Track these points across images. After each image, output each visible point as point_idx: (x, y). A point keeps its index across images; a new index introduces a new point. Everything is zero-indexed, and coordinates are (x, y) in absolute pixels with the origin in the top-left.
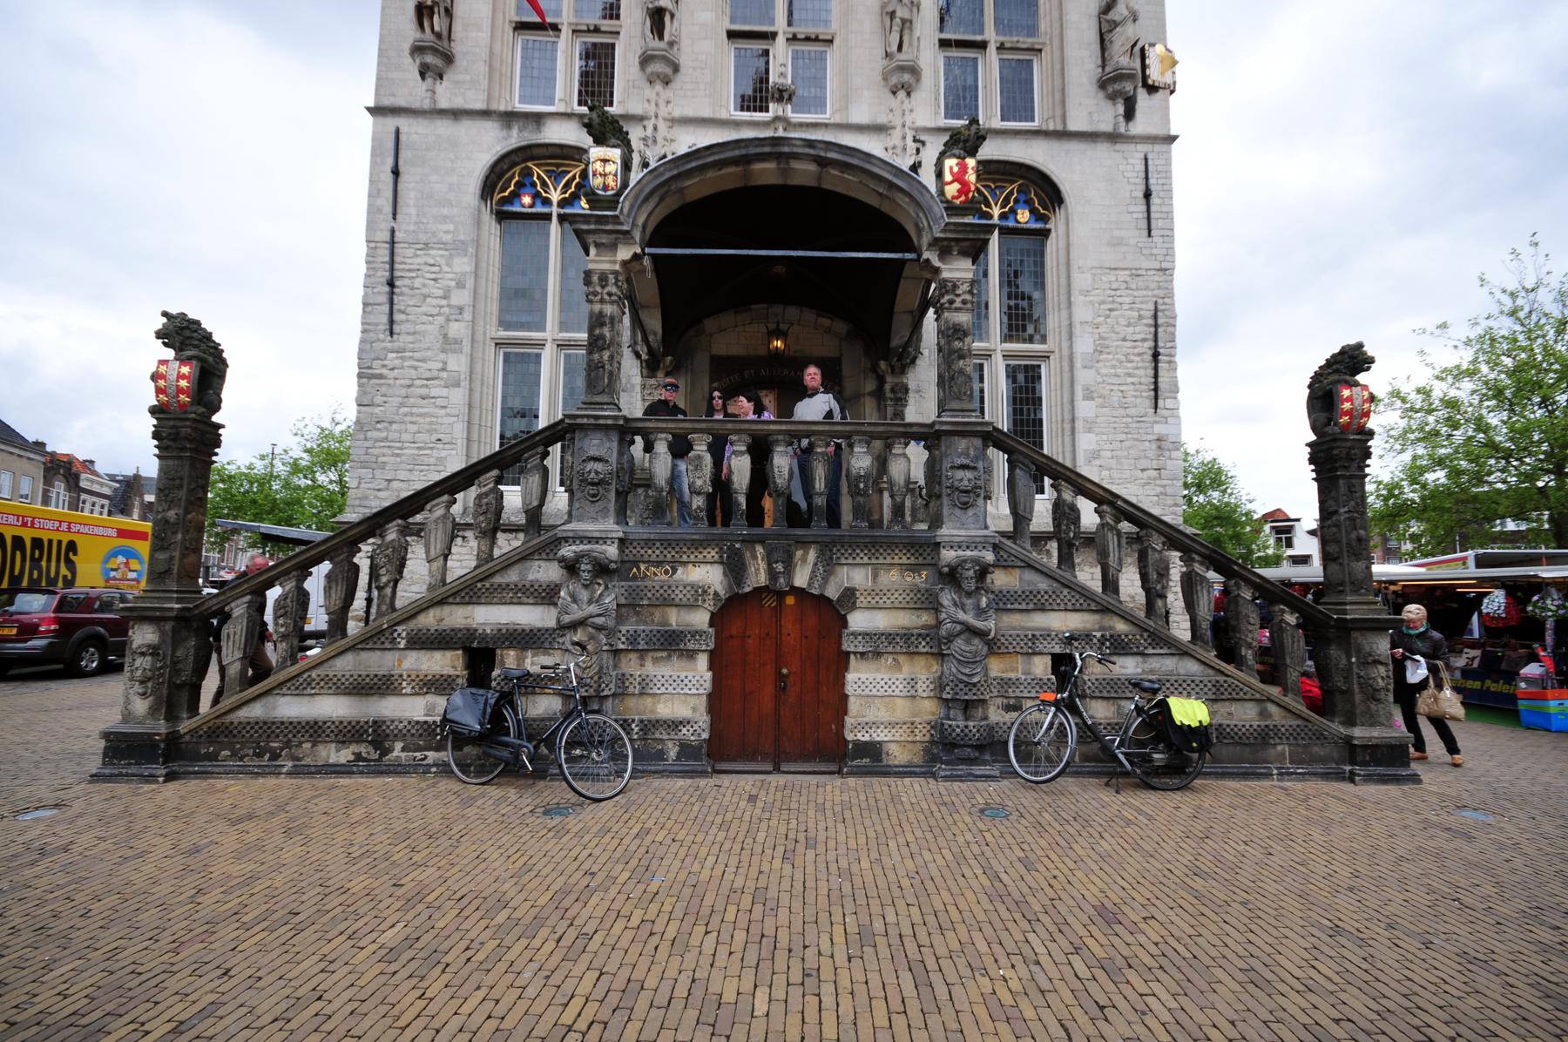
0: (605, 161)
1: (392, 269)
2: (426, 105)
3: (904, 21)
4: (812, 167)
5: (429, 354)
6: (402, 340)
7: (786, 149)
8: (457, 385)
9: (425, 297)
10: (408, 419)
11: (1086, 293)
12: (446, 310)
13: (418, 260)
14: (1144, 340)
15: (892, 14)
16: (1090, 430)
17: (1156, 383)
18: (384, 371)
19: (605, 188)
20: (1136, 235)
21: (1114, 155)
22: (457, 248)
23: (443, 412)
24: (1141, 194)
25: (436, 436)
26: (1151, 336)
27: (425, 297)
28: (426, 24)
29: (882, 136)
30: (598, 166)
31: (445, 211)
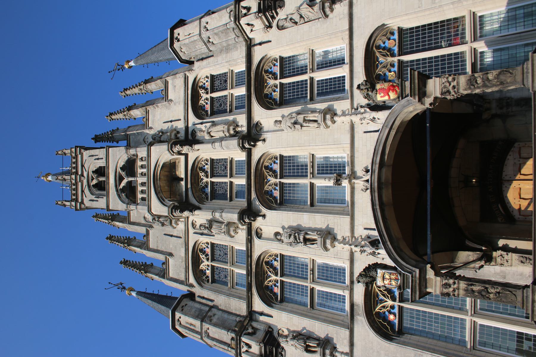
0: (384, 278)
4: (384, 170)
7: (376, 184)
29: (355, 126)
30: (386, 282)
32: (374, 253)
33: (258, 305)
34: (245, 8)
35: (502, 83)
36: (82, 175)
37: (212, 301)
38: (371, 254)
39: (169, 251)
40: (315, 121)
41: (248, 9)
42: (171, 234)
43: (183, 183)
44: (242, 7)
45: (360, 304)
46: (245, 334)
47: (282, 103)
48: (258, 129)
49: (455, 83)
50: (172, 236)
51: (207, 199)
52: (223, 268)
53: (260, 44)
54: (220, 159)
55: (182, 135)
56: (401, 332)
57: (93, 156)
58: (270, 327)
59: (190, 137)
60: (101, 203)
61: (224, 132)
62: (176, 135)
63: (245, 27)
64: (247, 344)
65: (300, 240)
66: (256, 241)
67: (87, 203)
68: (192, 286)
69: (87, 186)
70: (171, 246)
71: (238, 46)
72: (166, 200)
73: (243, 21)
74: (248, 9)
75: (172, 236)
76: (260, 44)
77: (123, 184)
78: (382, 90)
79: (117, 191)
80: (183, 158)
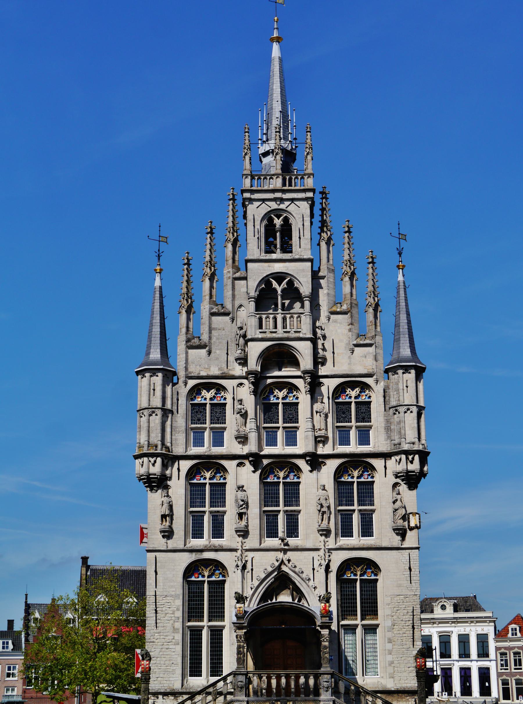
1: (156, 605)
2: (164, 548)
5: (168, 634)
6: (160, 629)
8: (178, 644)
9: (166, 614)
10: (163, 656)
11: (389, 604)
12: (173, 618)
13: (164, 601)
14: (409, 621)
16: (391, 654)
17: (413, 636)
18: (154, 640)
19: (240, 614)
20: (407, 583)
21: (398, 554)
22: (176, 597)
23: (174, 653)
24: (408, 568)
25: (171, 662)
26: (411, 619)
27: (166, 614)
28: (164, 520)
31: (172, 584)
32: (238, 566)
33: (186, 465)
34: (413, 458)
35: (324, 659)
36: (282, 200)
37: (178, 412)
38: (237, 564)
39: (213, 351)
40: (322, 520)
41: (412, 462)
42: (229, 353)
43: (276, 373)
44: (414, 456)
45: (203, 556)
49: (325, 640)
50: (227, 354)
51: (264, 399)
52: (206, 416)
53: (385, 467)
54: (298, 412)
56: (190, 583)
57: (303, 225)
58: (170, 478)
60: (254, 248)
61: (320, 430)
62: (320, 362)
63: (399, 457)
64: (155, 462)
65: (241, 509)
66: (236, 462)
67: (251, 209)
68: (186, 384)
69: (269, 209)
70: (218, 352)
71: (389, 441)
73: (403, 457)
74: (412, 462)
75: (227, 354)
76: (385, 467)
77: (275, 284)
78: (326, 606)
79: (267, 276)
80: (299, 373)
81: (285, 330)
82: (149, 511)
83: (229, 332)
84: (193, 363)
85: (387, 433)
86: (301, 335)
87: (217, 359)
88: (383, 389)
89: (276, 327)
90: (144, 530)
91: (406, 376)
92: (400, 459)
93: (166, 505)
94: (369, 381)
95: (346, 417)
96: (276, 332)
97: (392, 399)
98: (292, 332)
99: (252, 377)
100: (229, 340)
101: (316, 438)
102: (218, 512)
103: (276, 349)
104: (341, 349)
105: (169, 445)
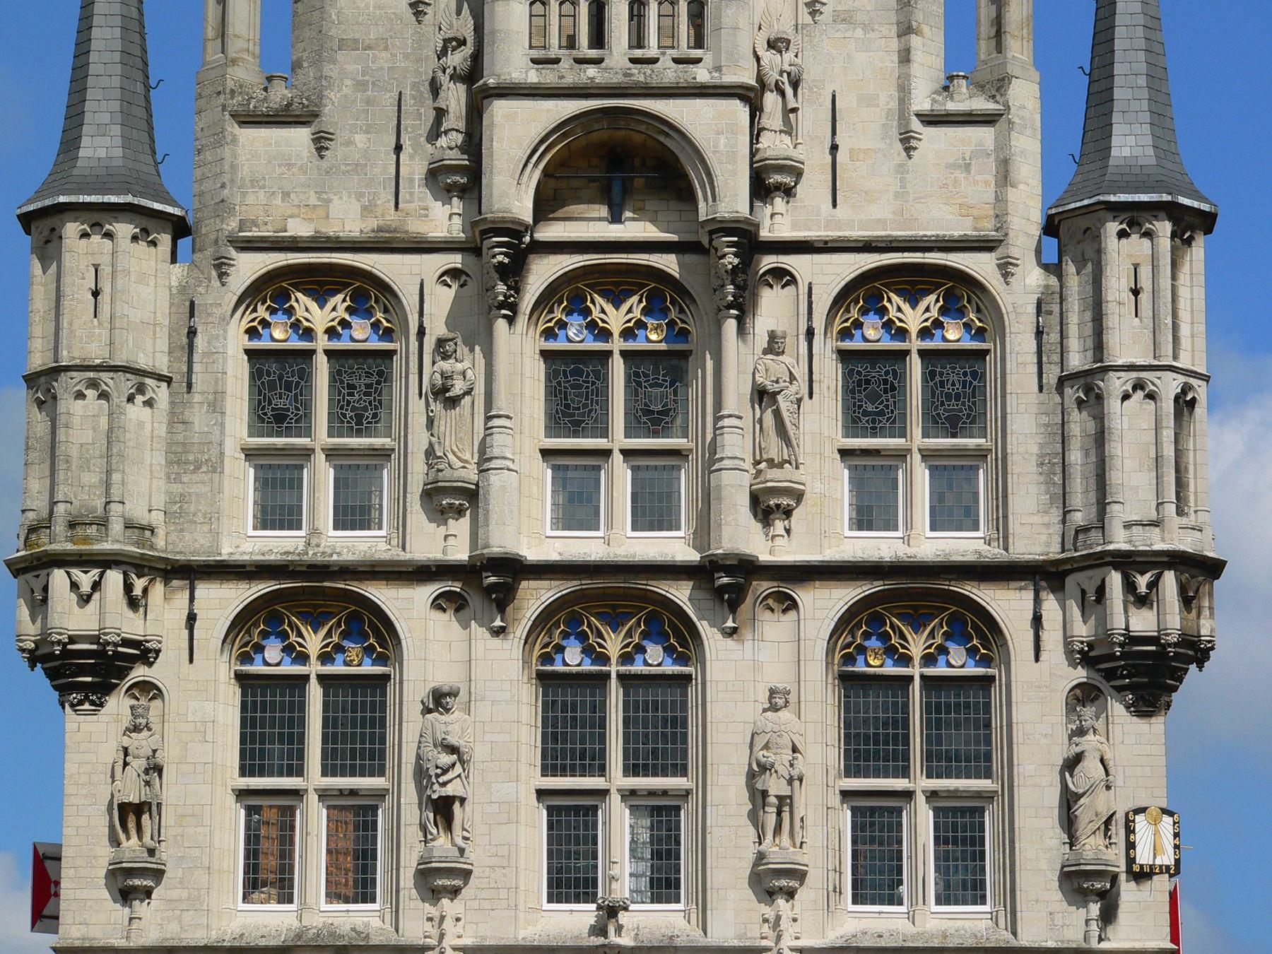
3: (780, 798)
15: (765, 794)
28: (132, 825)
33: (222, 602)
34: (1153, 585)
39: (341, 136)
42: (406, 141)
46: (125, 574)
47: (851, 683)
48: (770, 601)
50: (398, 148)
53: (1037, 620)
55: (778, 222)
58: (158, 652)
59: (768, 261)
62: (778, 187)
63: (1096, 574)
71: (1056, 515)
72: (537, 174)
75: (398, 148)
76: (1037, 620)
81: (638, 53)
82: (69, 789)
83: (406, 56)
84: (254, 182)
85: (1049, 482)
86: (702, 75)
87: (358, 168)
88: (1034, 298)
89: (598, 39)
90: (48, 864)
91: (1137, 246)
92: (1101, 591)
93: (138, 764)
94: (980, 265)
95: (881, 413)
96: (598, 61)
97: (1074, 343)
98: (666, 62)
99: (500, 245)
100: (408, 92)
101: (755, 499)
102: (353, 793)
103: (602, 134)
104: (866, 132)
105: (157, 518)
